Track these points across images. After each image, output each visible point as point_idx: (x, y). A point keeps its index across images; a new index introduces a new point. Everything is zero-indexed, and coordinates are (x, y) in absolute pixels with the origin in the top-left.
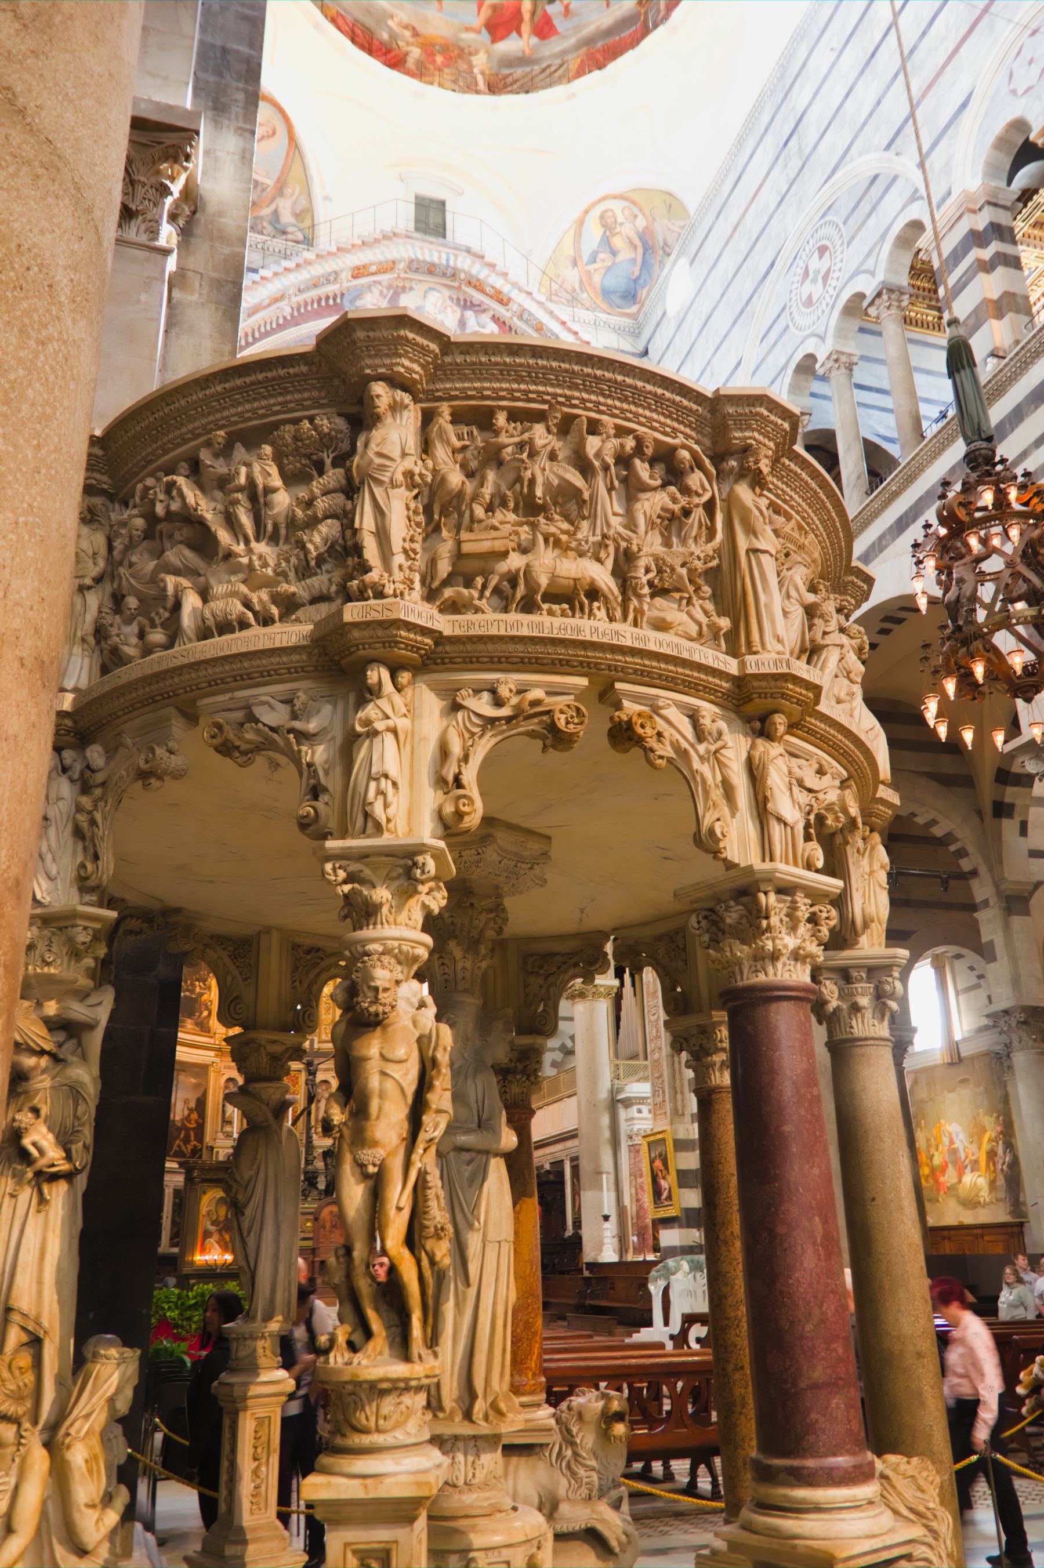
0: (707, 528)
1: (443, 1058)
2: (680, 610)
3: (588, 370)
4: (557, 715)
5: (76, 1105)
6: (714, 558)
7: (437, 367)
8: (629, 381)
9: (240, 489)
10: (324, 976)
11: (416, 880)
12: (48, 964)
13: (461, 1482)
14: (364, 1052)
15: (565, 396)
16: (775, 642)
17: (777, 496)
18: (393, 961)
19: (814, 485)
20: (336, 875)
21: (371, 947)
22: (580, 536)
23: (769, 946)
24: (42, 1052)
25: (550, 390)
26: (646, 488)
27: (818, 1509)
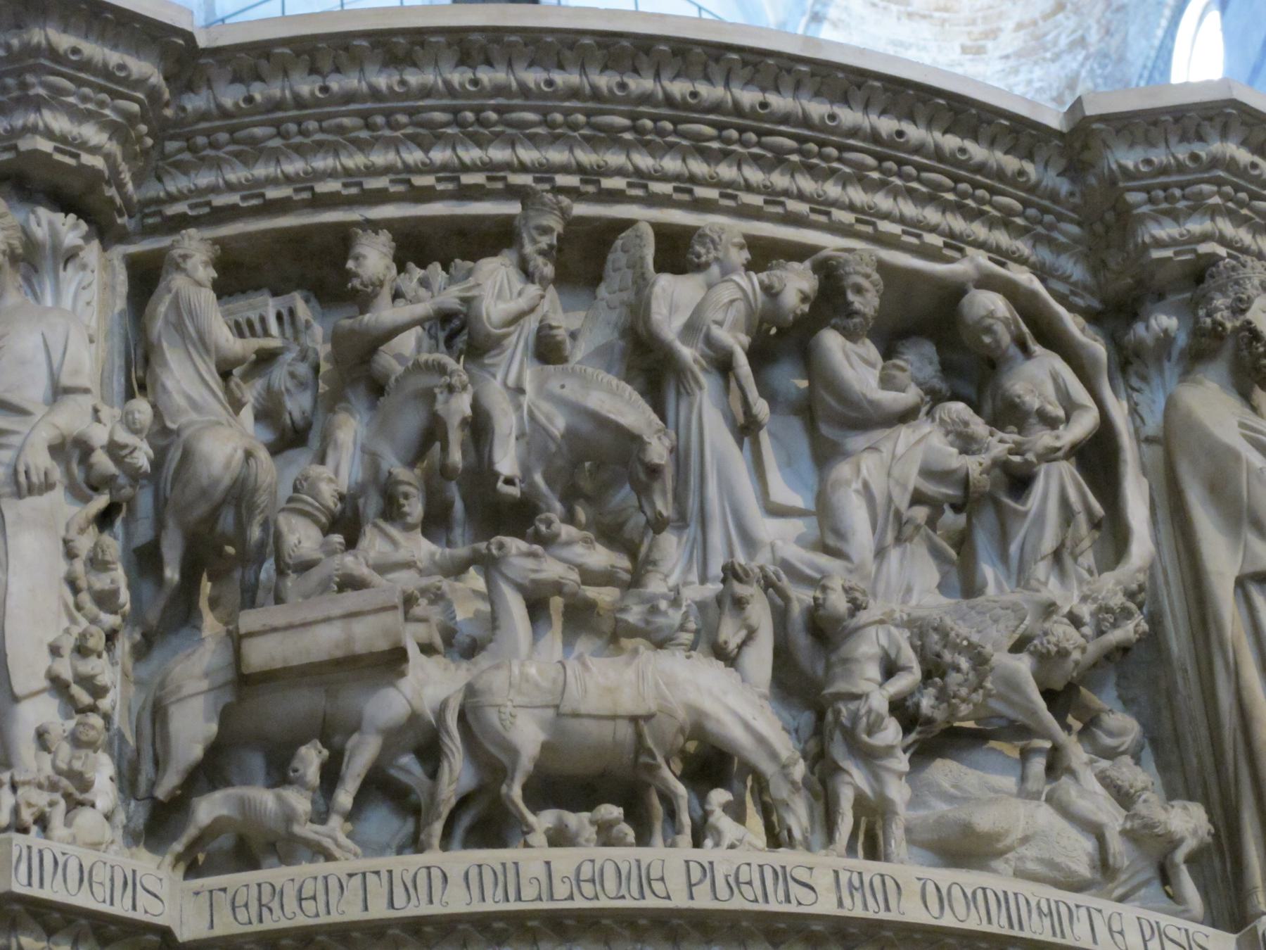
0: (1095, 525)
2: (1025, 794)
3: (642, 84)
6: (1126, 614)
7: (162, 131)
8: (780, 102)
15: (580, 169)
22: (656, 585)
25: (528, 155)
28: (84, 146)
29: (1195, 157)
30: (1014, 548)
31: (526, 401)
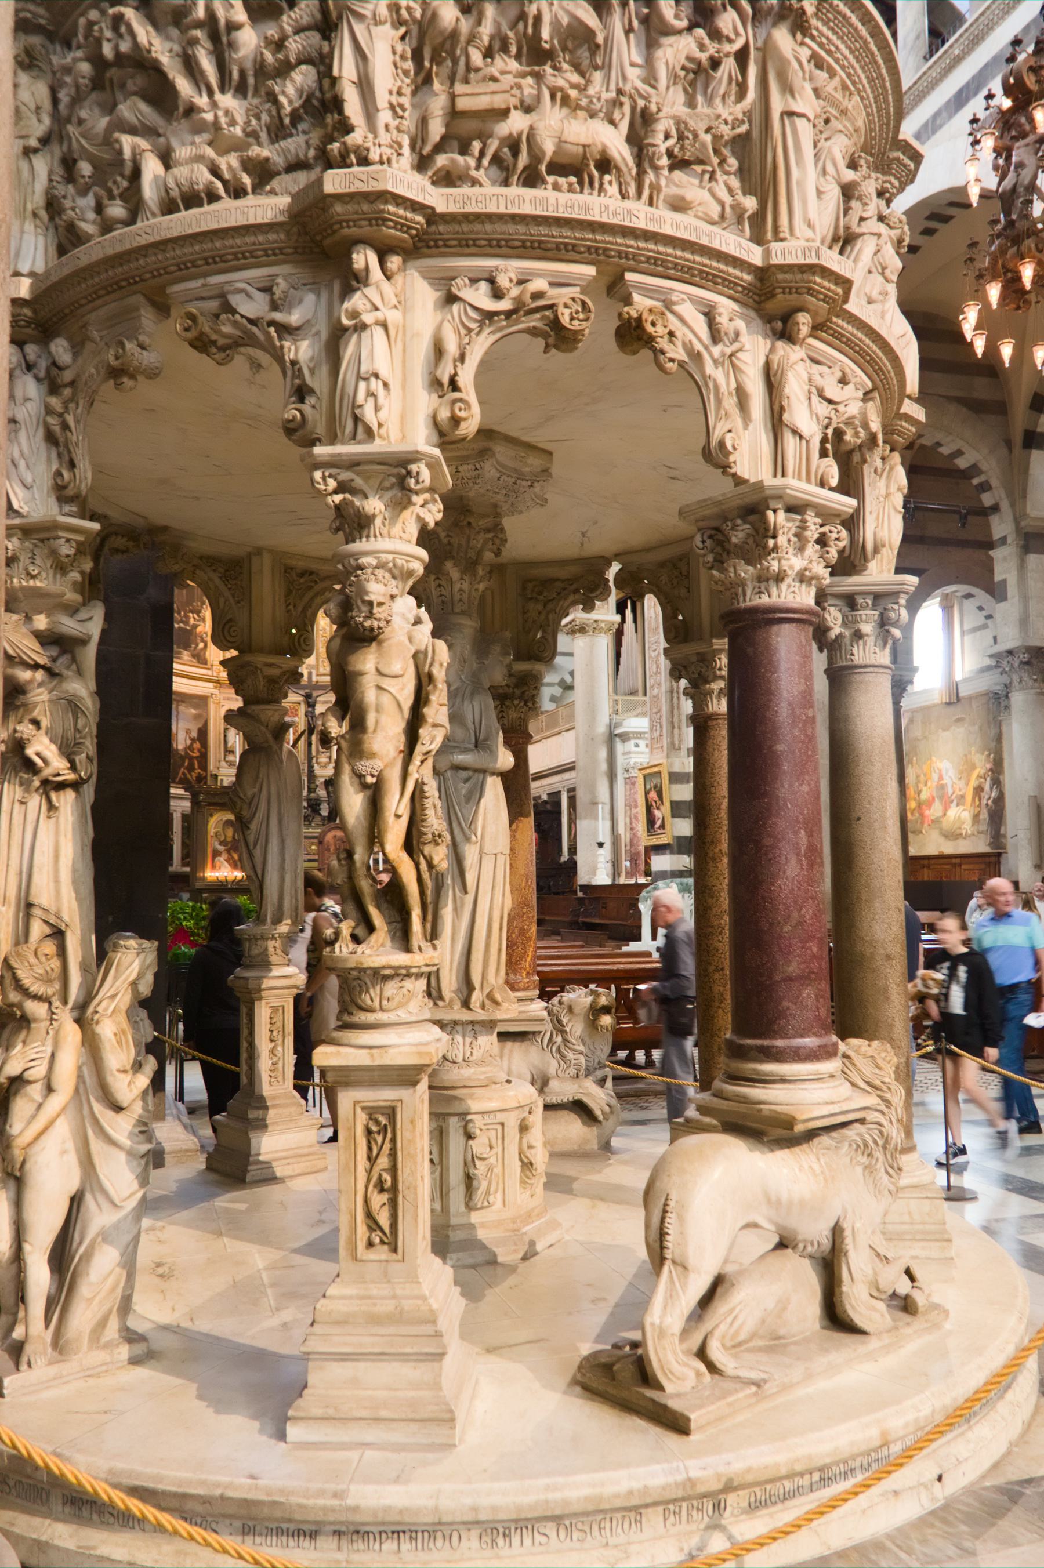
0: (738, 84)
1: (439, 674)
2: (702, 187)
4: (561, 309)
5: (76, 719)
6: (743, 122)
9: (199, 25)
10: (318, 600)
11: (410, 490)
12: (33, 577)
13: (460, 1059)
14: (359, 667)
16: (805, 227)
17: (821, 45)
18: (387, 575)
19: (864, 31)
20: (326, 484)
21: (364, 560)
22: (591, 91)
23: (775, 566)
24: (36, 666)
26: (669, 31)
27: (783, 1080)
30: (710, 91)
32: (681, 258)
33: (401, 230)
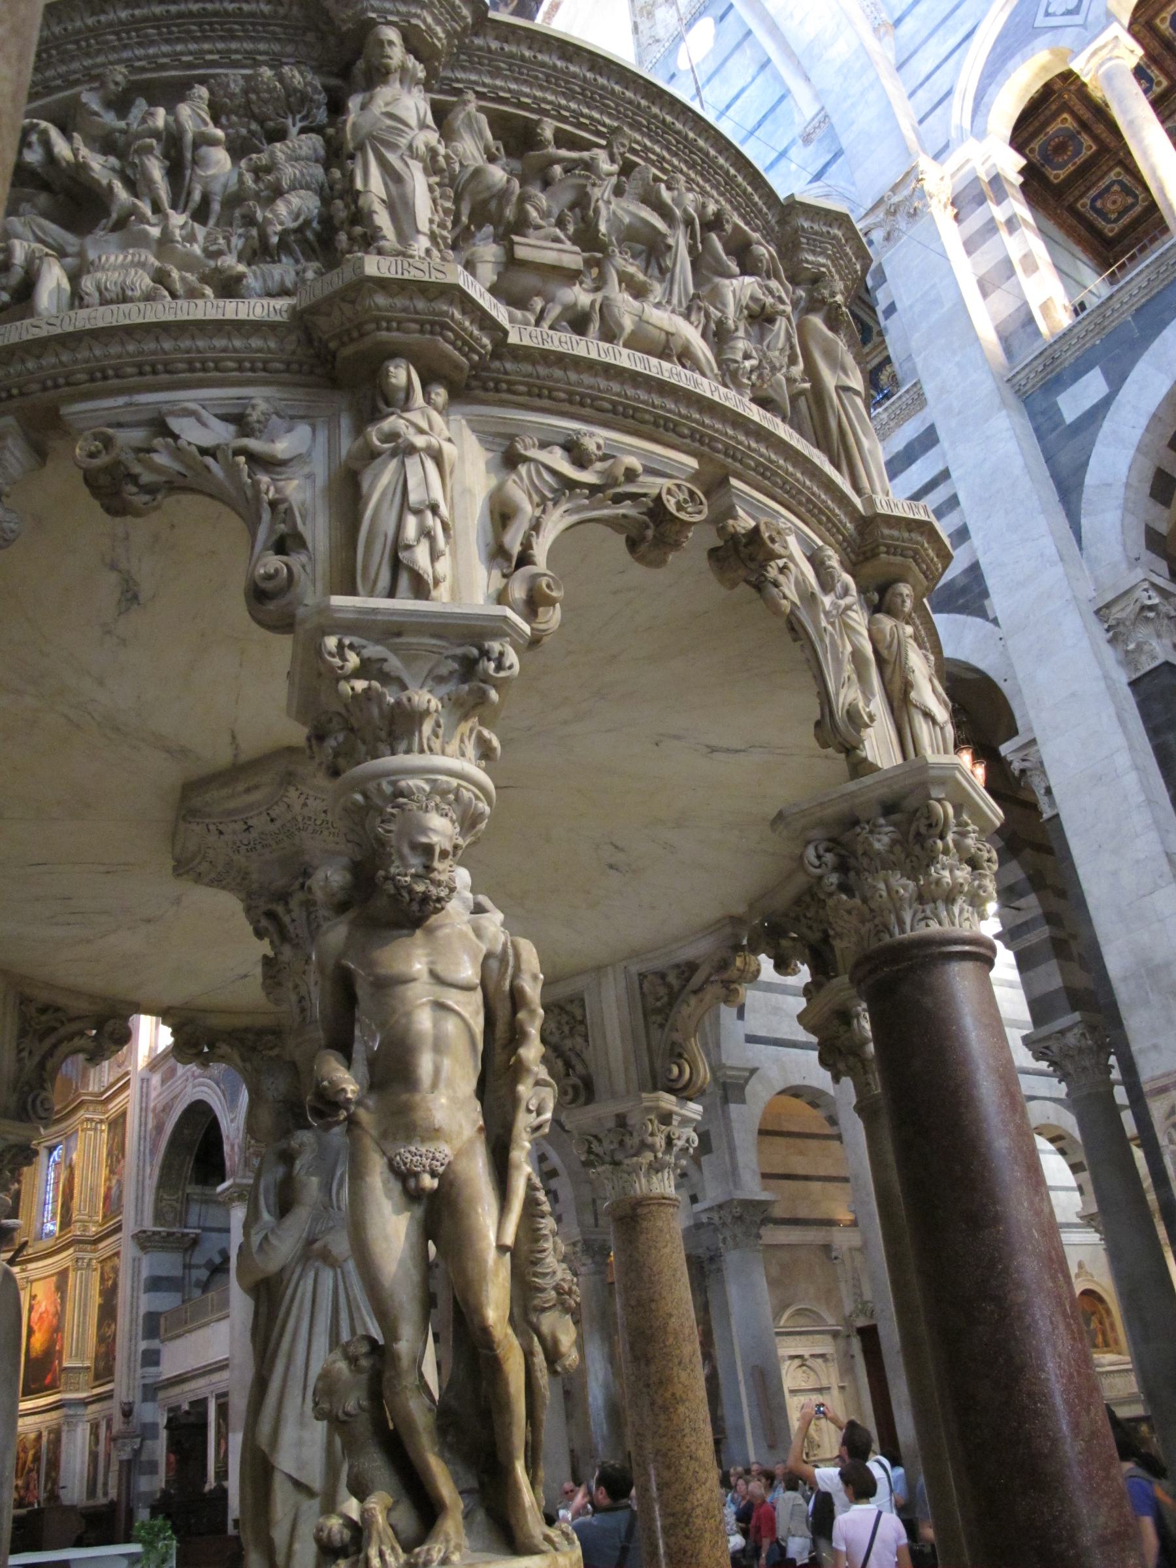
4: (664, 496)
7: (462, 48)
9: (155, 134)
10: (65, 1047)
11: (487, 679)
14: (398, 968)
20: (344, 659)
21: (413, 783)
28: (436, 34)
29: (828, 232)
31: (613, 207)
32: (791, 475)
33: (460, 350)
